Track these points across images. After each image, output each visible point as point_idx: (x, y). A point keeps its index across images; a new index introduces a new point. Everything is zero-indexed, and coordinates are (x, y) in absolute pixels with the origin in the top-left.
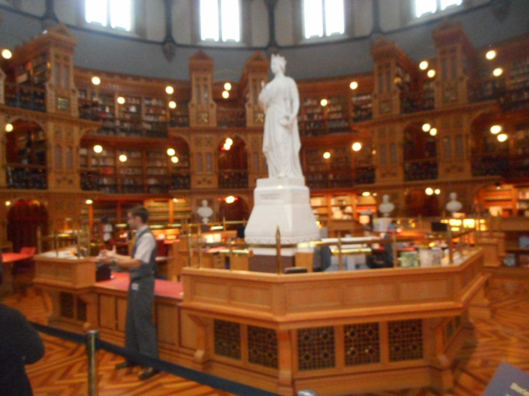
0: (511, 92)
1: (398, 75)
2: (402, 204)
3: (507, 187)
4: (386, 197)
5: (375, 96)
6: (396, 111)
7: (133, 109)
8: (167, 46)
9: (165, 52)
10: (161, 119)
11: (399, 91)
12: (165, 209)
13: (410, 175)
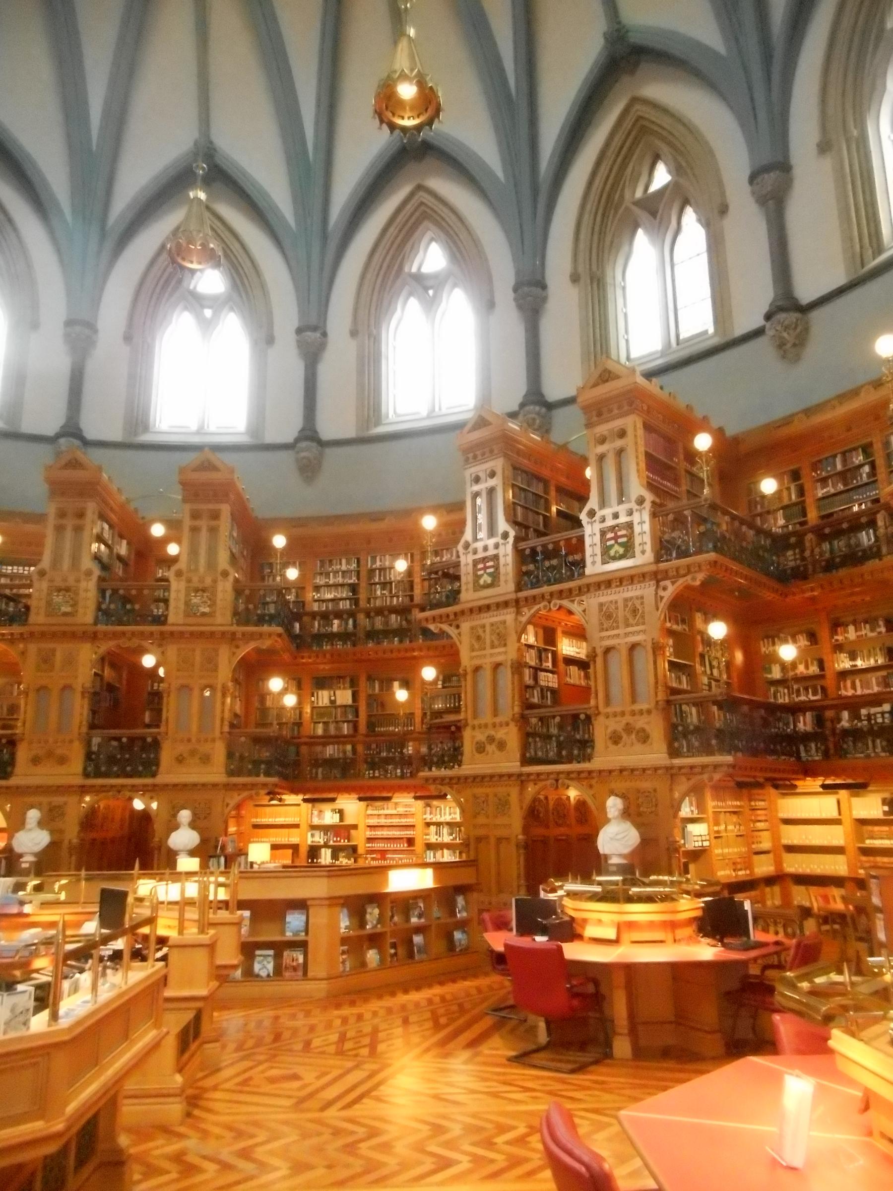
0: (313, 615)
1: (100, 539)
2: (72, 833)
3: (290, 798)
4: (33, 815)
5: (42, 573)
6: (87, 615)
11: (97, 572)
13: (96, 765)
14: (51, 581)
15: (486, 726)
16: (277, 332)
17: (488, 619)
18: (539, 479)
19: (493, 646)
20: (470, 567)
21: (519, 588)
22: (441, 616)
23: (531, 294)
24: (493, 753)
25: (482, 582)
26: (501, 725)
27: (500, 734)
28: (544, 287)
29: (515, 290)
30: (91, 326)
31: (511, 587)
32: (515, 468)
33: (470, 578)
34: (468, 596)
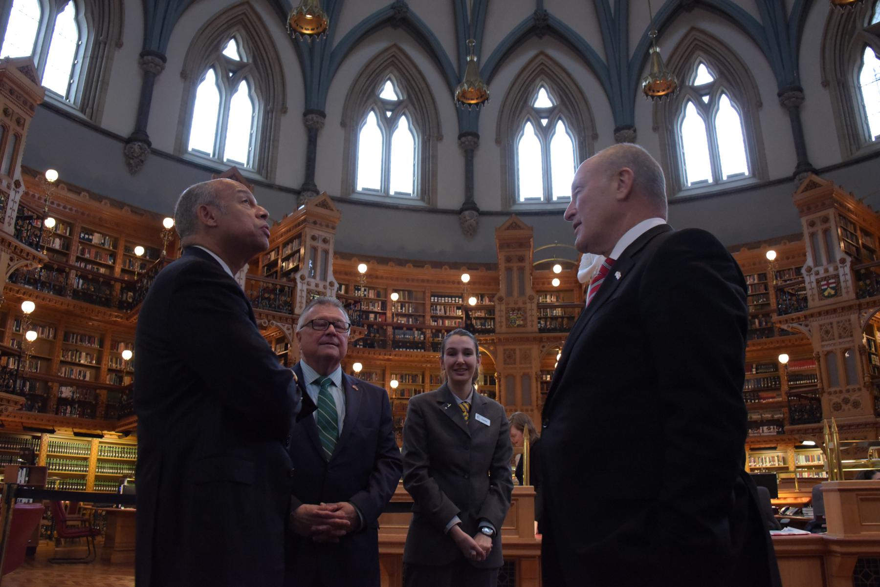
5: (501, 299)
7: (57, 244)
8: (136, 147)
9: (128, 156)
10: (102, 270)
12: (82, 453)
14: (507, 304)
15: (841, 392)
16: (599, 131)
17: (834, 319)
18: (851, 223)
19: (840, 337)
20: (814, 285)
21: (858, 297)
22: (793, 319)
23: (792, 97)
24: (849, 409)
25: (826, 294)
26: (854, 390)
27: (854, 397)
28: (801, 90)
29: (780, 95)
30: (476, 136)
31: (853, 295)
32: (840, 215)
33: (815, 291)
34: (814, 303)
